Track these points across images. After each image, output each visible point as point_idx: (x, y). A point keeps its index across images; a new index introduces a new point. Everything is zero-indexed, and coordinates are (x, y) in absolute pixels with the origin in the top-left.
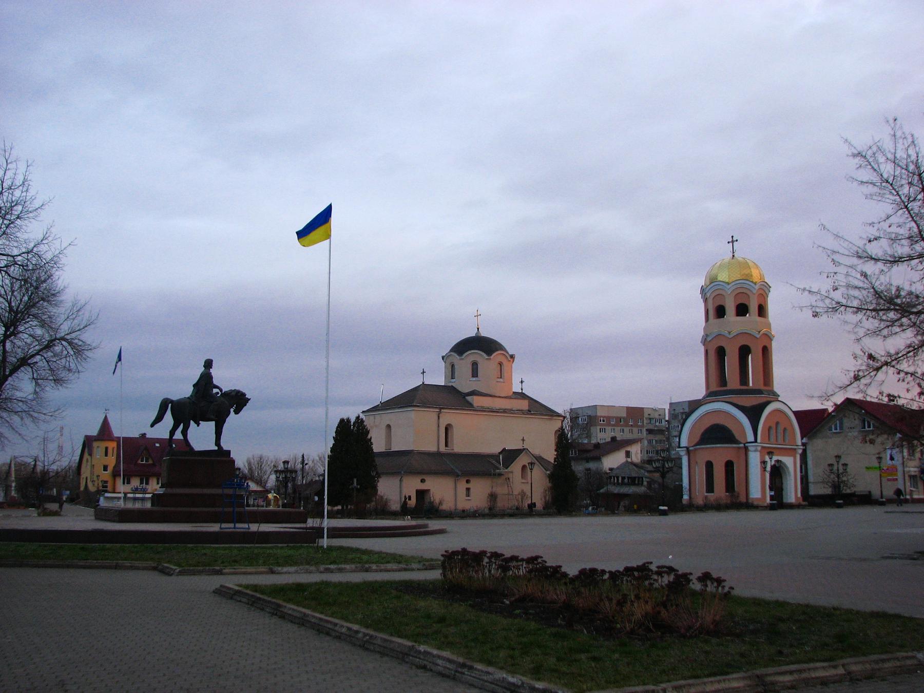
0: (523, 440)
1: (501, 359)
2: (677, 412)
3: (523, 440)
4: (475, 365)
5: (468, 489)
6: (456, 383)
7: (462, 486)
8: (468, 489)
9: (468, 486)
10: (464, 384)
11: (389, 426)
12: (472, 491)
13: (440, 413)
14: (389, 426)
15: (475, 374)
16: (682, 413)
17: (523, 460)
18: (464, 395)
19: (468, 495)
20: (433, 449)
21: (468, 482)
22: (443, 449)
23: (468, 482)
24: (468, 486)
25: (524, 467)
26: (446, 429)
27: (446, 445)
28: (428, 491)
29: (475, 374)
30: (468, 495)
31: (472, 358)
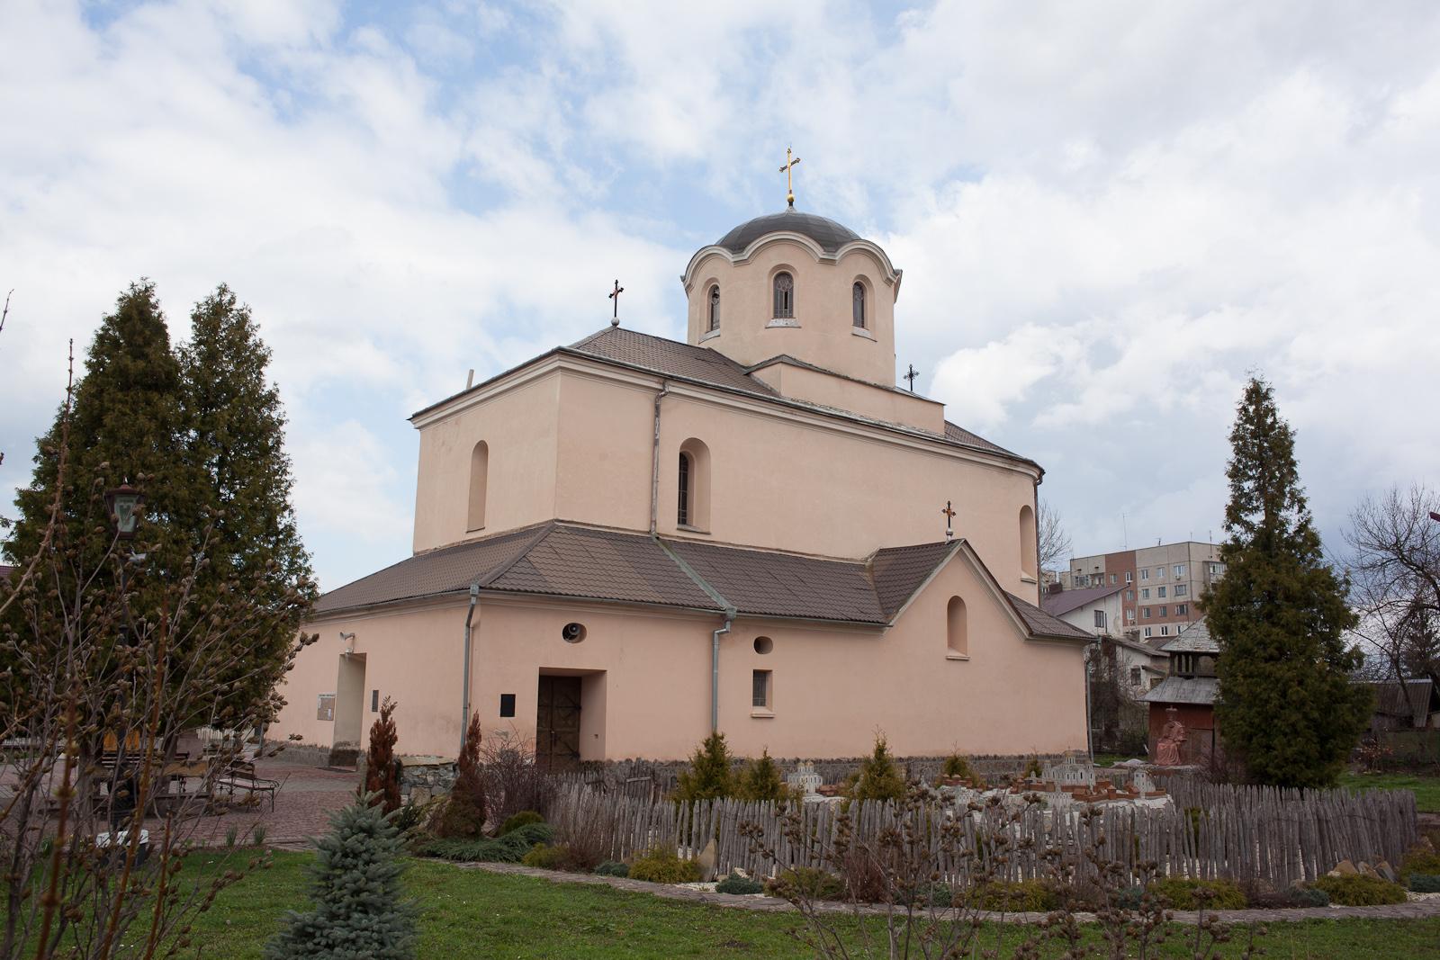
0: (949, 513)
1: (865, 267)
2: (1084, 573)
3: (949, 513)
4: (783, 277)
5: (761, 677)
6: (720, 343)
7: (739, 660)
8: (761, 677)
9: (762, 661)
10: (748, 334)
11: (482, 448)
12: (776, 685)
13: (660, 395)
14: (482, 448)
15: (783, 304)
16: (1093, 576)
17: (949, 580)
18: (748, 372)
19: (760, 696)
20: (636, 522)
21: (761, 646)
22: (668, 524)
23: (761, 646)
24: (762, 661)
25: (955, 604)
26: (685, 462)
27: (683, 518)
28: (597, 675)
29: (783, 304)
30: (760, 696)
31: (775, 258)
